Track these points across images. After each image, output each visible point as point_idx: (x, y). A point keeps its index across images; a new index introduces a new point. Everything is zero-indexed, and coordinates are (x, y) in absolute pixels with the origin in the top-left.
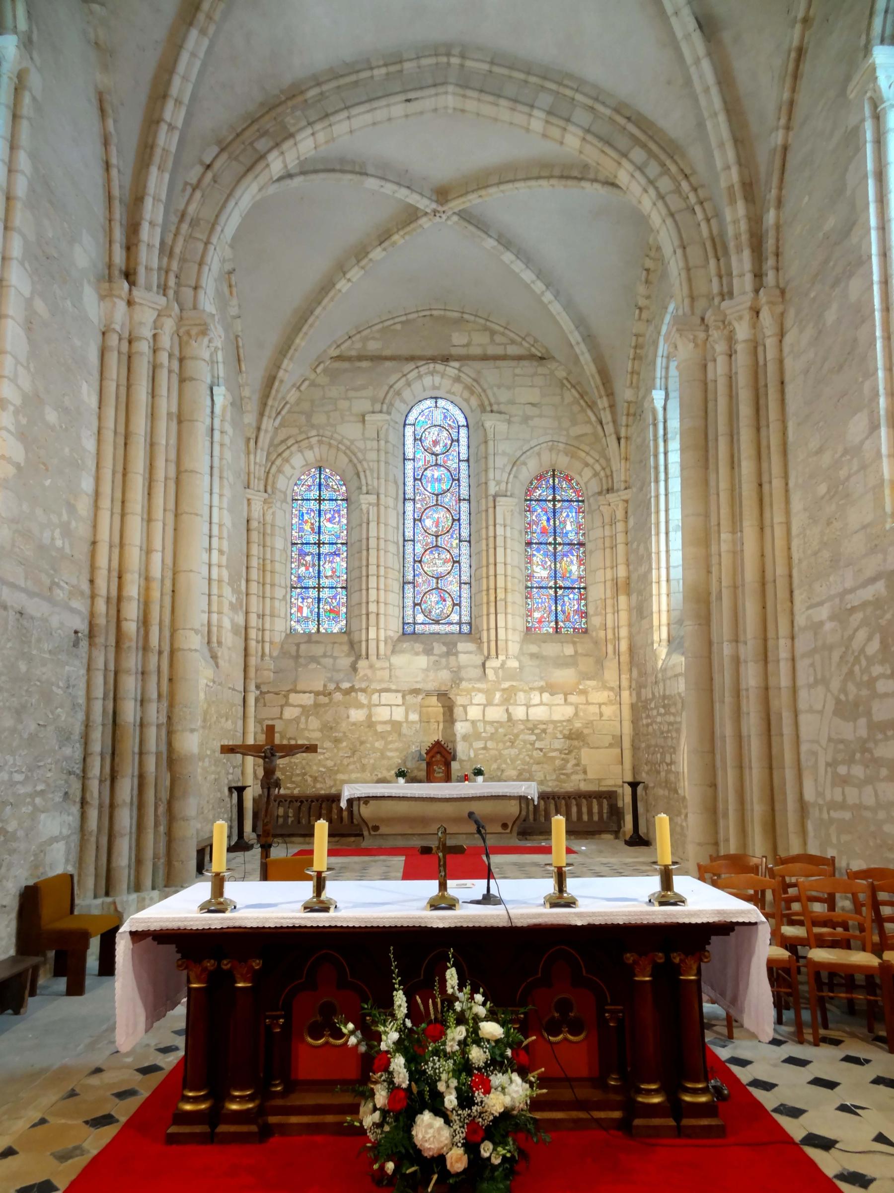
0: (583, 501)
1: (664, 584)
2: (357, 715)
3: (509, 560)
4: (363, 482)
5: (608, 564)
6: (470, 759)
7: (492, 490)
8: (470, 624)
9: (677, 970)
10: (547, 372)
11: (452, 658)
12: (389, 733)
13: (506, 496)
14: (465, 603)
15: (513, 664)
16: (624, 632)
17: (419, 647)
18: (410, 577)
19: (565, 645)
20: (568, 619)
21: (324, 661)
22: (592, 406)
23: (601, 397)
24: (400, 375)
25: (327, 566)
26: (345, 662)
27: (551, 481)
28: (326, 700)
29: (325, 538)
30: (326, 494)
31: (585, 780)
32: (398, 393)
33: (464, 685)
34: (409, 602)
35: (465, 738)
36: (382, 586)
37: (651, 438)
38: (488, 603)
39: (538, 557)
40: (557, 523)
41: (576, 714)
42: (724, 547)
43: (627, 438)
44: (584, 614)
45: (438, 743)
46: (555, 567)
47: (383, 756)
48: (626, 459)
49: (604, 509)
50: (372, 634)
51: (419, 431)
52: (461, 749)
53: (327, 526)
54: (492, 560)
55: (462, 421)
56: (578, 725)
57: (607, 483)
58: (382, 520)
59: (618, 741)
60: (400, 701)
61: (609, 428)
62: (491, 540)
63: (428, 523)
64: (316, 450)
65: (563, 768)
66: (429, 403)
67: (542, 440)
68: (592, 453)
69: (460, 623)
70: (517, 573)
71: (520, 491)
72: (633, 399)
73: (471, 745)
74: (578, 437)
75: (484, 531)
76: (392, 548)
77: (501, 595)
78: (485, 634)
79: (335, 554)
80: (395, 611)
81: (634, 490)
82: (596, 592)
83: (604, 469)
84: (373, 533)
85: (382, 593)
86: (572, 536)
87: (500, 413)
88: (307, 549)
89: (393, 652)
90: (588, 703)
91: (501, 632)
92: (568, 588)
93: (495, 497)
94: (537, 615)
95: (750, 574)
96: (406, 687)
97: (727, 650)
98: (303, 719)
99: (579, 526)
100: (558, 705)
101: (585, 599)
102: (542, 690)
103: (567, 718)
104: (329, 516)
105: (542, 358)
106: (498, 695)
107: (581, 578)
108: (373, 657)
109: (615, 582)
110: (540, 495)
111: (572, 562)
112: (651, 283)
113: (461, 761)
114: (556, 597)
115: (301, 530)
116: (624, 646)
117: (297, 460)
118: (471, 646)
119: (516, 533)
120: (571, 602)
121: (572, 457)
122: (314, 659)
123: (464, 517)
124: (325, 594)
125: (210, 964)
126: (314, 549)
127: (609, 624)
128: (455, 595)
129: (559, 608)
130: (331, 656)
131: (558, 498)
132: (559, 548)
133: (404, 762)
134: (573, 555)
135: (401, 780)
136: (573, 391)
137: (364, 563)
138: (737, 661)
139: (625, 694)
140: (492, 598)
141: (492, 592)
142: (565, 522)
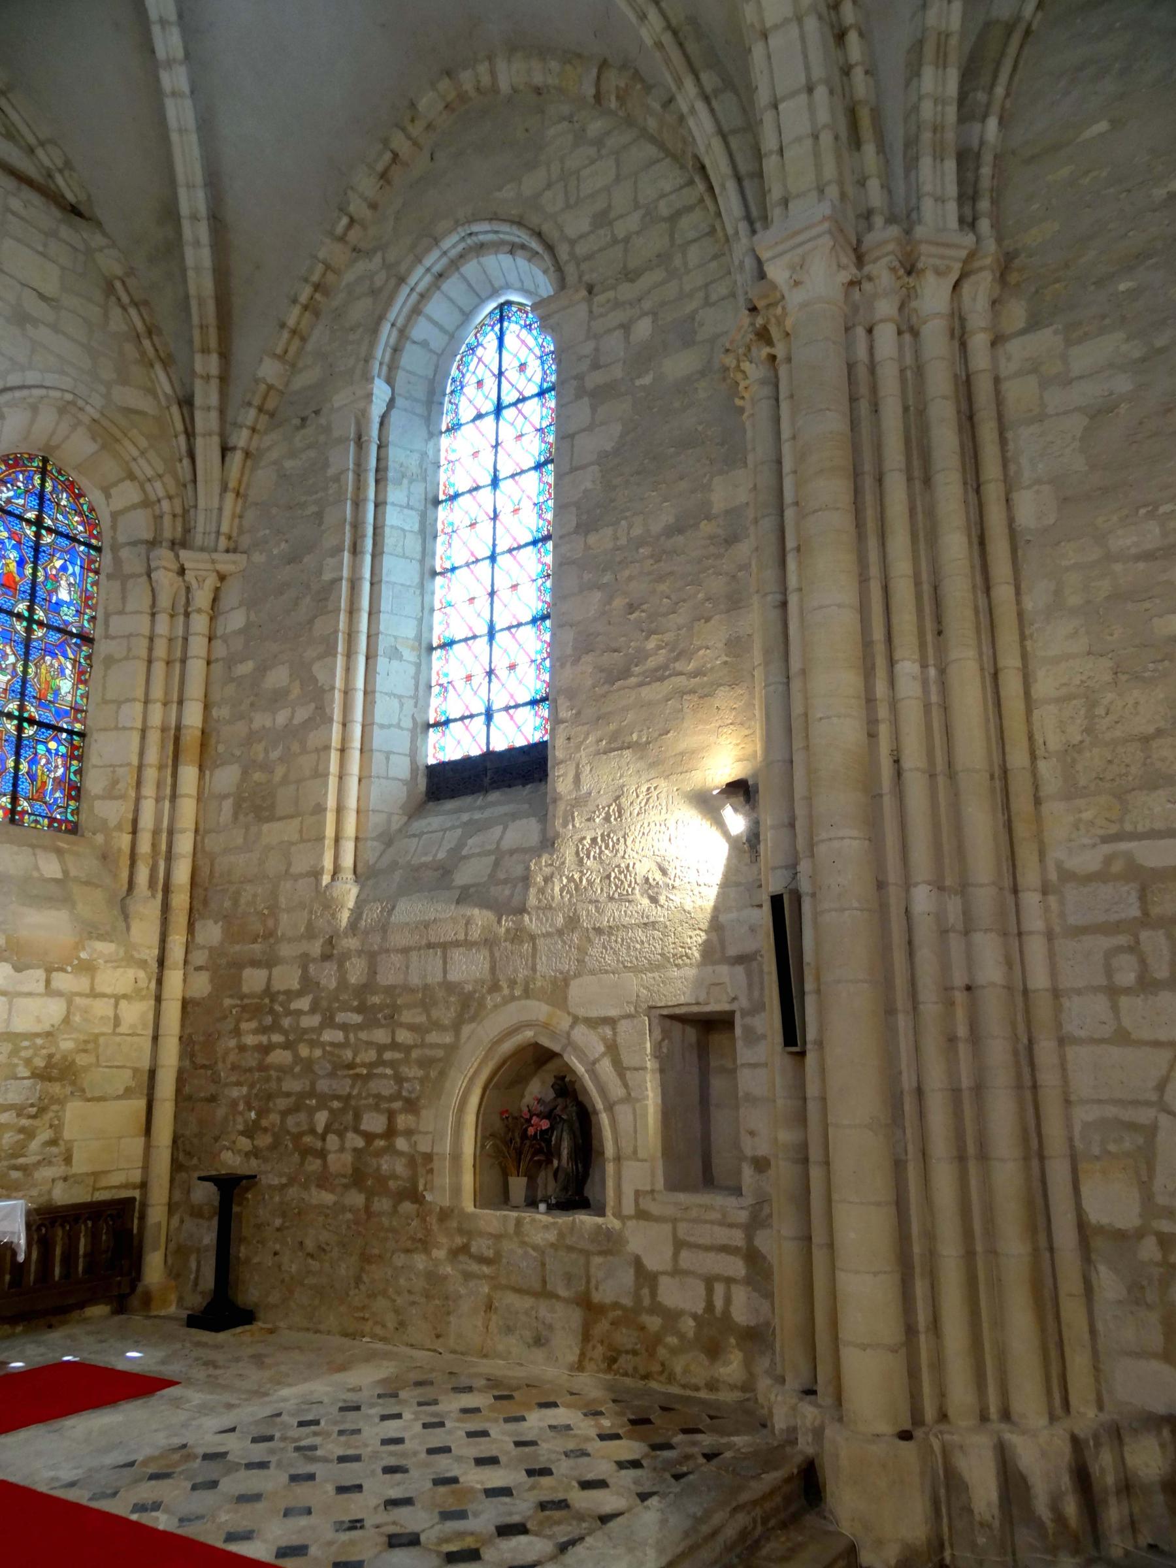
0: (98, 549)
1: (355, 756)
5: (157, 692)
16: (185, 844)
19: (38, 851)
20: (39, 796)
23: (205, 350)
27: (37, 481)
31: (65, 1179)
37: (351, 466)
40: (41, 574)
41: (67, 1020)
43: (247, 454)
46: (25, 672)
48: (238, 494)
49: (165, 579)
56: (67, 1044)
57: (174, 528)
65: (19, 1150)
67: (50, 379)
68: (151, 454)
72: (279, 384)
74: (128, 411)
81: (259, 558)
82: (102, 749)
83: (170, 498)
86: (68, 615)
90: (94, 994)
92: (49, 726)
100: (30, 994)
101: (80, 759)
103: (47, 1028)
105: (75, 211)
107: (77, 710)
110: (9, 501)
111: (62, 671)
112: (389, 182)
114: (19, 738)
116: (182, 874)
121: (104, 447)
127: (147, 820)
129: (24, 767)
131: (48, 522)
134: (66, 657)
136: (133, 312)
142: (56, 578)
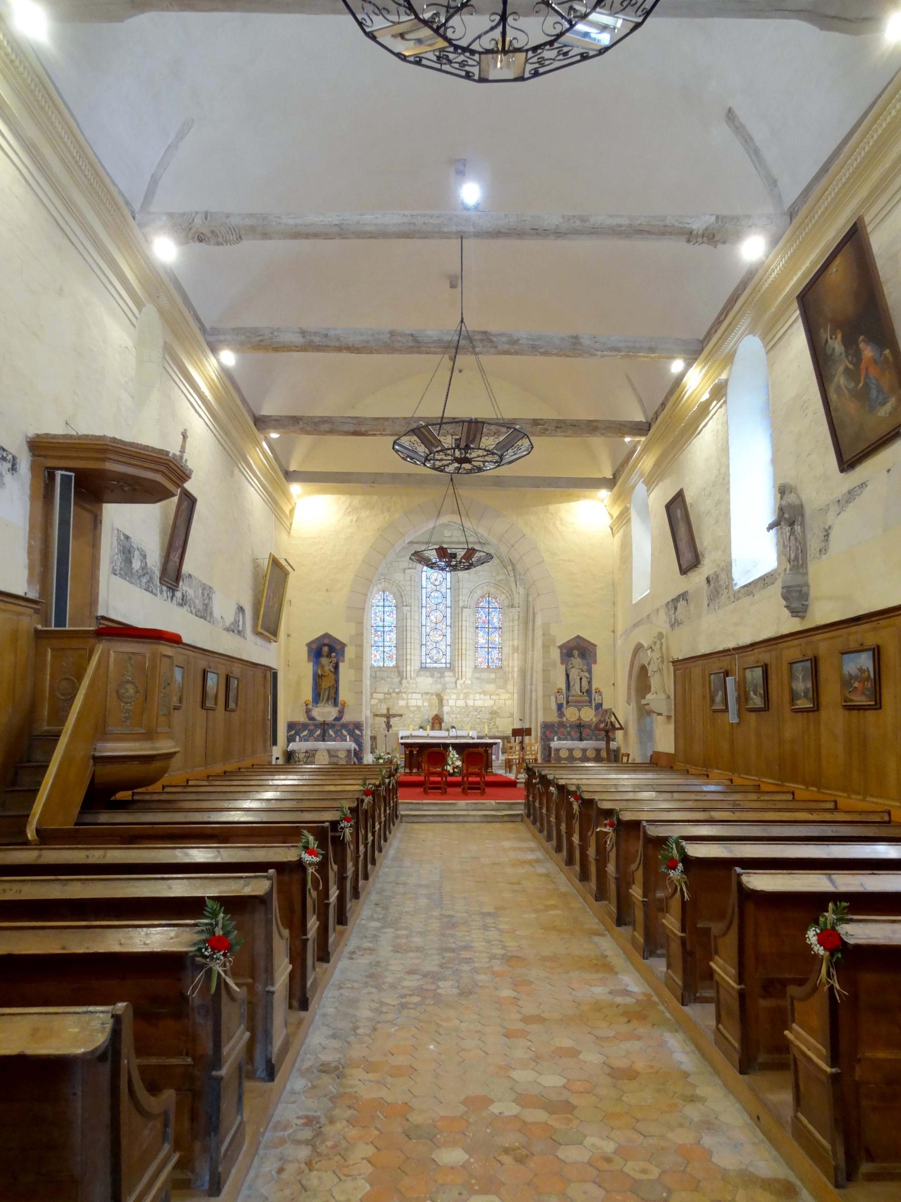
2: (402, 703)
8: (450, 663)
11: (442, 679)
14: (448, 654)
15: (468, 682)
17: (428, 674)
18: (424, 643)
21: (388, 679)
22: (505, 567)
25: (388, 637)
26: (397, 680)
28: (389, 696)
29: (386, 624)
30: (387, 603)
33: (448, 691)
34: (423, 653)
39: (481, 634)
44: (501, 660)
45: (436, 715)
47: (413, 721)
49: (510, 614)
50: (408, 667)
52: (446, 718)
53: (387, 618)
59: (512, 715)
61: (513, 579)
63: (432, 618)
64: (383, 584)
69: (446, 663)
70: (471, 641)
71: (473, 604)
74: (499, 581)
76: (416, 630)
77: (464, 652)
79: (390, 631)
80: (417, 657)
82: (506, 650)
84: (409, 624)
86: (496, 625)
88: (378, 629)
93: (463, 608)
94: (480, 660)
97: (529, 687)
99: (500, 620)
102: (480, 693)
106: (462, 695)
108: (409, 679)
109: (513, 646)
115: (376, 620)
116: (516, 675)
117: (376, 589)
118: (451, 674)
120: (495, 654)
122: (382, 678)
123: (449, 615)
124: (387, 649)
126: (381, 629)
127: (510, 665)
128: (444, 651)
135: (421, 730)
138: (531, 691)
139: (516, 696)
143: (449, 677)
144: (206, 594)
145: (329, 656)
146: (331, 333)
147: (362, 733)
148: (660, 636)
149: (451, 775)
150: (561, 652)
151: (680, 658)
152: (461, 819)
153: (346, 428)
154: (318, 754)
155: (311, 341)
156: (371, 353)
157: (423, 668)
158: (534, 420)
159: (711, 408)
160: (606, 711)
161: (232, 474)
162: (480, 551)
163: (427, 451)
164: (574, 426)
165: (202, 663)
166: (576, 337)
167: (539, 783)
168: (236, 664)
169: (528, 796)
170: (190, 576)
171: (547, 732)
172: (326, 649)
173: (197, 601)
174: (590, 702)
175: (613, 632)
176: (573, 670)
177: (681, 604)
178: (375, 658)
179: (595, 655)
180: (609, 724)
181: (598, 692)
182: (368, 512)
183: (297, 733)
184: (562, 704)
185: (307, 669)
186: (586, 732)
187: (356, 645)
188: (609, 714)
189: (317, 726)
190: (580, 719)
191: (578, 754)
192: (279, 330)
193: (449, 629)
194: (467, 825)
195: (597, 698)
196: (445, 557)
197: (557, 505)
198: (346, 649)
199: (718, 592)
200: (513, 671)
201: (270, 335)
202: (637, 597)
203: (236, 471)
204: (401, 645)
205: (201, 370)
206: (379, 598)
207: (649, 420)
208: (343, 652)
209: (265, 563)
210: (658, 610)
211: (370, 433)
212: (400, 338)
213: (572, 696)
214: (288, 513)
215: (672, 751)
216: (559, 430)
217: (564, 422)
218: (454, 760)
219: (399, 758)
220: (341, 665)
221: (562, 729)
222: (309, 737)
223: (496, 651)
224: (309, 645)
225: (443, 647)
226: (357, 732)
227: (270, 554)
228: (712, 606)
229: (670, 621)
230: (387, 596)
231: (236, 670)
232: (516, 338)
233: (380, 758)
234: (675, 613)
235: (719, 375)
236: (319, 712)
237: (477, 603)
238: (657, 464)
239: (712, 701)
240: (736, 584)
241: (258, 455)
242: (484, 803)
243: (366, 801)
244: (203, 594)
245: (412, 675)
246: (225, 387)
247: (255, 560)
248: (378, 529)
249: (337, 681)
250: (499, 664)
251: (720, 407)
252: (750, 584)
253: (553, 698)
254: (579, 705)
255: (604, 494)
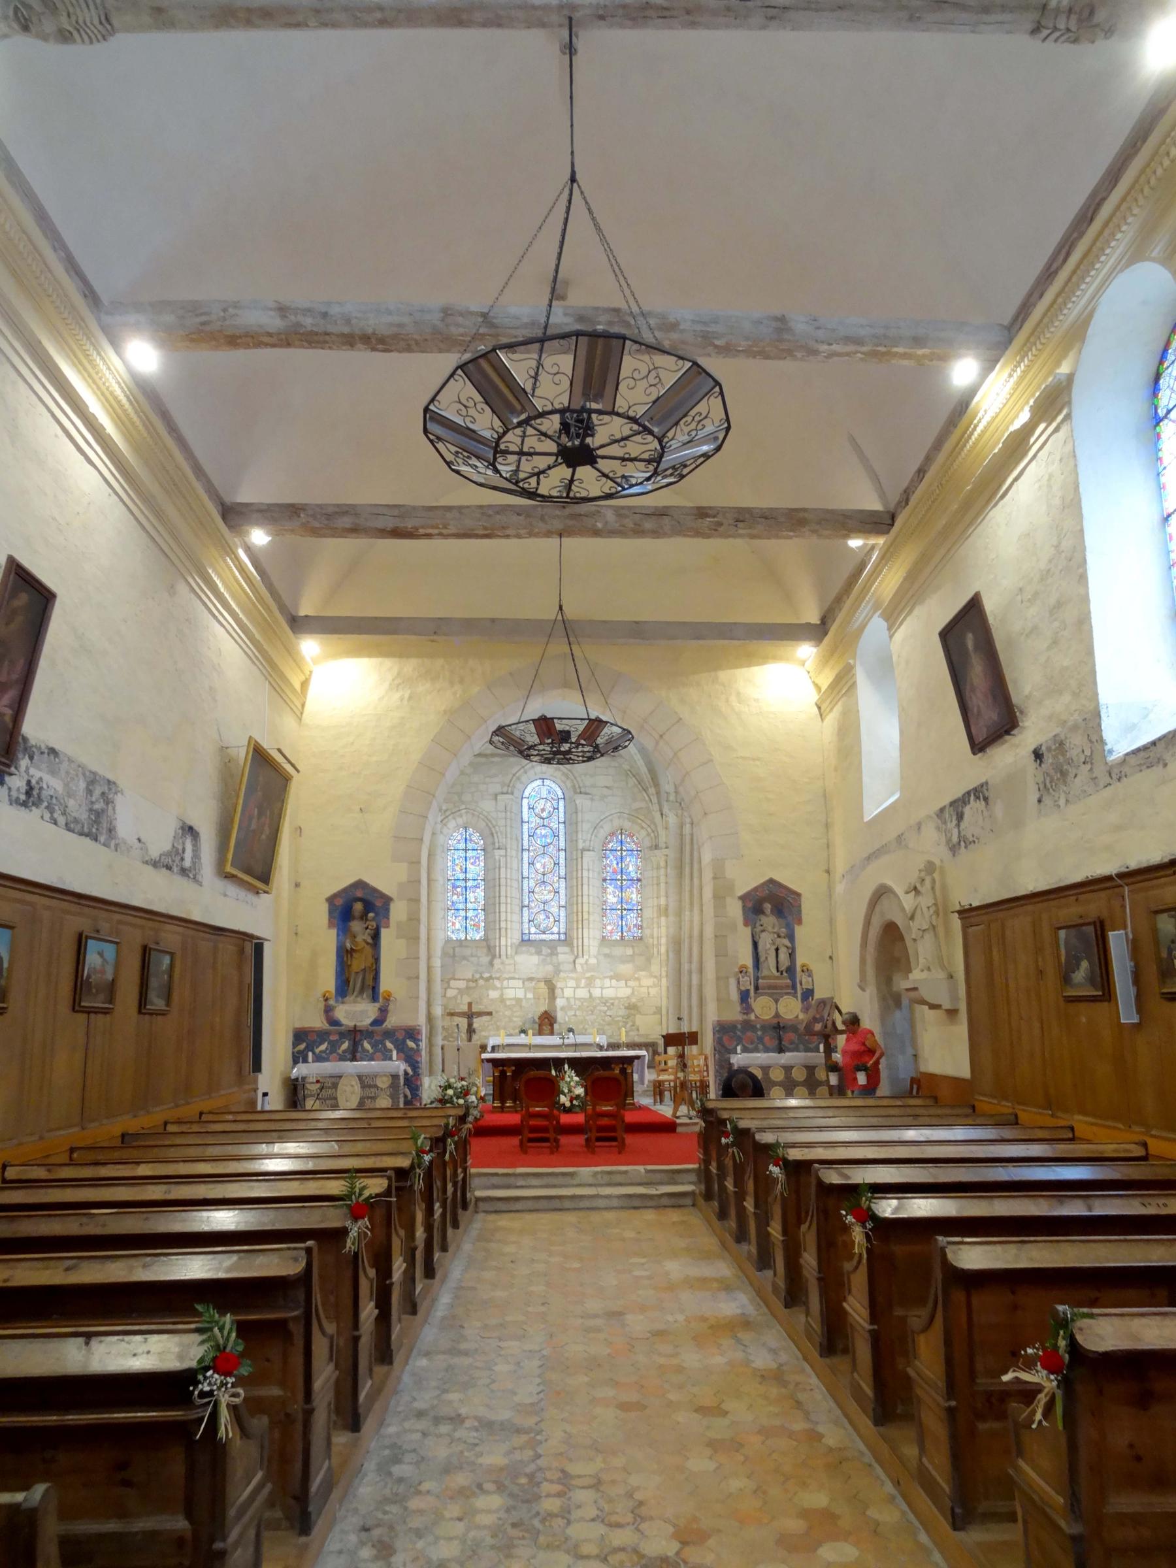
2: (494, 994)
3: (591, 893)
4: (496, 840)
5: (655, 895)
6: (566, 1022)
7: (581, 845)
8: (565, 934)
9: (626, 1069)
10: (617, 765)
11: (554, 957)
12: (514, 1006)
13: (589, 850)
14: (563, 920)
15: (593, 961)
17: (533, 950)
18: (526, 903)
20: (629, 930)
22: (645, 790)
24: (520, 767)
26: (485, 960)
28: (474, 984)
29: (469, 876)
32: (519, 779)
33: (562, 975)
34: (526, 919)
35: (562, 1009)
36: (509, 910)
38: (577, 921)
39: (611, 889)
41: (633, 993)
42: (687, 918)
45: (546, 1012)
48: (666, 828)
49: (653, 859)
51: (532, 802)
52: (560, 1016)
53: (470, 867)
54: (580, 893)
55: (560, 795)
56: (634, 1000)
58: (509, 866)
59: (658, 1011)
60: (521, 986)
61: (656, 807)
62: (580, 879)
63: (538, 866)
66: (539, 782)
69: (559, 933)
73: (566, 1014)
74: (637, 810)
75: (575, 873)
76: (515, 884)
77: (585, 916)
78: (575, 941)
79: (476, 887)
80: (516, 926)
82: (648, 913)
84: (503, 876)
85: (509, 914)
86: (633, 875)
87: (586, 794)
88: (458, 883)
89: (516, 953)
90: (640, 986)
91: (586, 940)
94: (609, 928)
95: (696, 933)
96: (525, 977)
97: (686, 967)
98: (459, 997)
102: (611, 978)
104: (472, 861)
106: (583, 981)
108: (504, 957)
109: (659, 906)
111: (632, 892)
113: (560, 1024)
115: (454, 870)
116: (663, 949)
117: (452, 824)
118: (566, 949)
119: (596, 874)
120: (632, 919)
122: (464, 958)
123: (562, 861)
124: (470, 914)
125: (501, 1068)
126: (462, 884)
127: (655, 935)
130: (476, 956)
132: (624, 883)
133: (524, 1024)
135: (523, 1035)
137: (497, 894)
138: (690, 972)
139: (664, 981)
140: (580, 918)
141: (580, 914)
143: (564, 956)
144: (97, 792)
145: (363, 917)
146: (335, 310)
147: (418, 1045)
148: (930, 868)
149: (568, 1111)
150: (744, 907)
151: (975, 904)
152: (583, 1204)
153: (380, 523)
154: (342, 1081)
155: (299, 325)
156: (409, 349)
157: (525, 942)
158: (698, 508)
159: (1032, 440)
160: (823, 1003)
161: (171, 590)
162: (612, 724)
163: (497, 423)
164: (766, 518)
165: (78, 921)
166: (782, 319)
167: (733, 1144)
168: (168, 927)
169: (707, 1162)
170: (53, 751)
171: (725, 1038)
172: (358, 907)
173: (71, 803)
174: (794, 987)
175: (828, 872)
176: (763, 935)
177: (973, 809)
178: (453, 927)
179: (800, 911)
180: (829, 1024)
181: (806, 970)
182: (428, 685)
183: (309, 1048)
184: (748, 991)
185: (327, 940)
186: (789, 1036)
187: (410, 900)
188: (828, 1007)
189: (343, 1035)
190: (777, 1015)
191: (777, 1075)
192: (236, 305)
193: (563, 883)
194: (596, 1217)
195: (804, 981)
196: (550, 735)
197: (729, 671)
198: (393, 906)
199: (1064, 774)
200: (659, 944)
201: (222, 314)
202: (871, 811)
203: (182, 588)
204: (491, 907)
205: (90, 376)
206: (459, 838)
207: (892, 507)
208: (387, 910)
209: (241, 754)
210: (919, 826)
211: (422, 531)
212: (460, 320)
213: (764, 978)
214: (297, 686)
215: (965, 1072)
216: (740, 525)
217: (749, 510)
218: (572, 1086)
219: (482, 1086)
220: (384, 933)
221: (749, 1034)
222: (331, 1053)
223: (633, 915)
224: (331, 900)
225: (555, 910)
226: (411, 1044)
227: (250, 737)
228: (1047, 800)
229: (949, 841)
230: (470, 835)
231: (171, 937)
232: (672, 319)
233: (450, 1086)
234: (958, 825)
235: (1058, 364)
236: (346, 1012)
237: (605, 844)
238: (912, 577)
239: (1066, 980)
240: (1111, 751)
241: (231, 570)
242: (626, 1172)
243: (353, 1234)
244: (89, 792)
245: (509, 953)
246: (148, 425)
247: (223, 749)
248: (445, 712)
249: (377, 959)
250: (638, 933)
251: (1057, 430)
252: (1154, 743)
253: (732, 982)
254: (776, 993)
255: (806, 651)
